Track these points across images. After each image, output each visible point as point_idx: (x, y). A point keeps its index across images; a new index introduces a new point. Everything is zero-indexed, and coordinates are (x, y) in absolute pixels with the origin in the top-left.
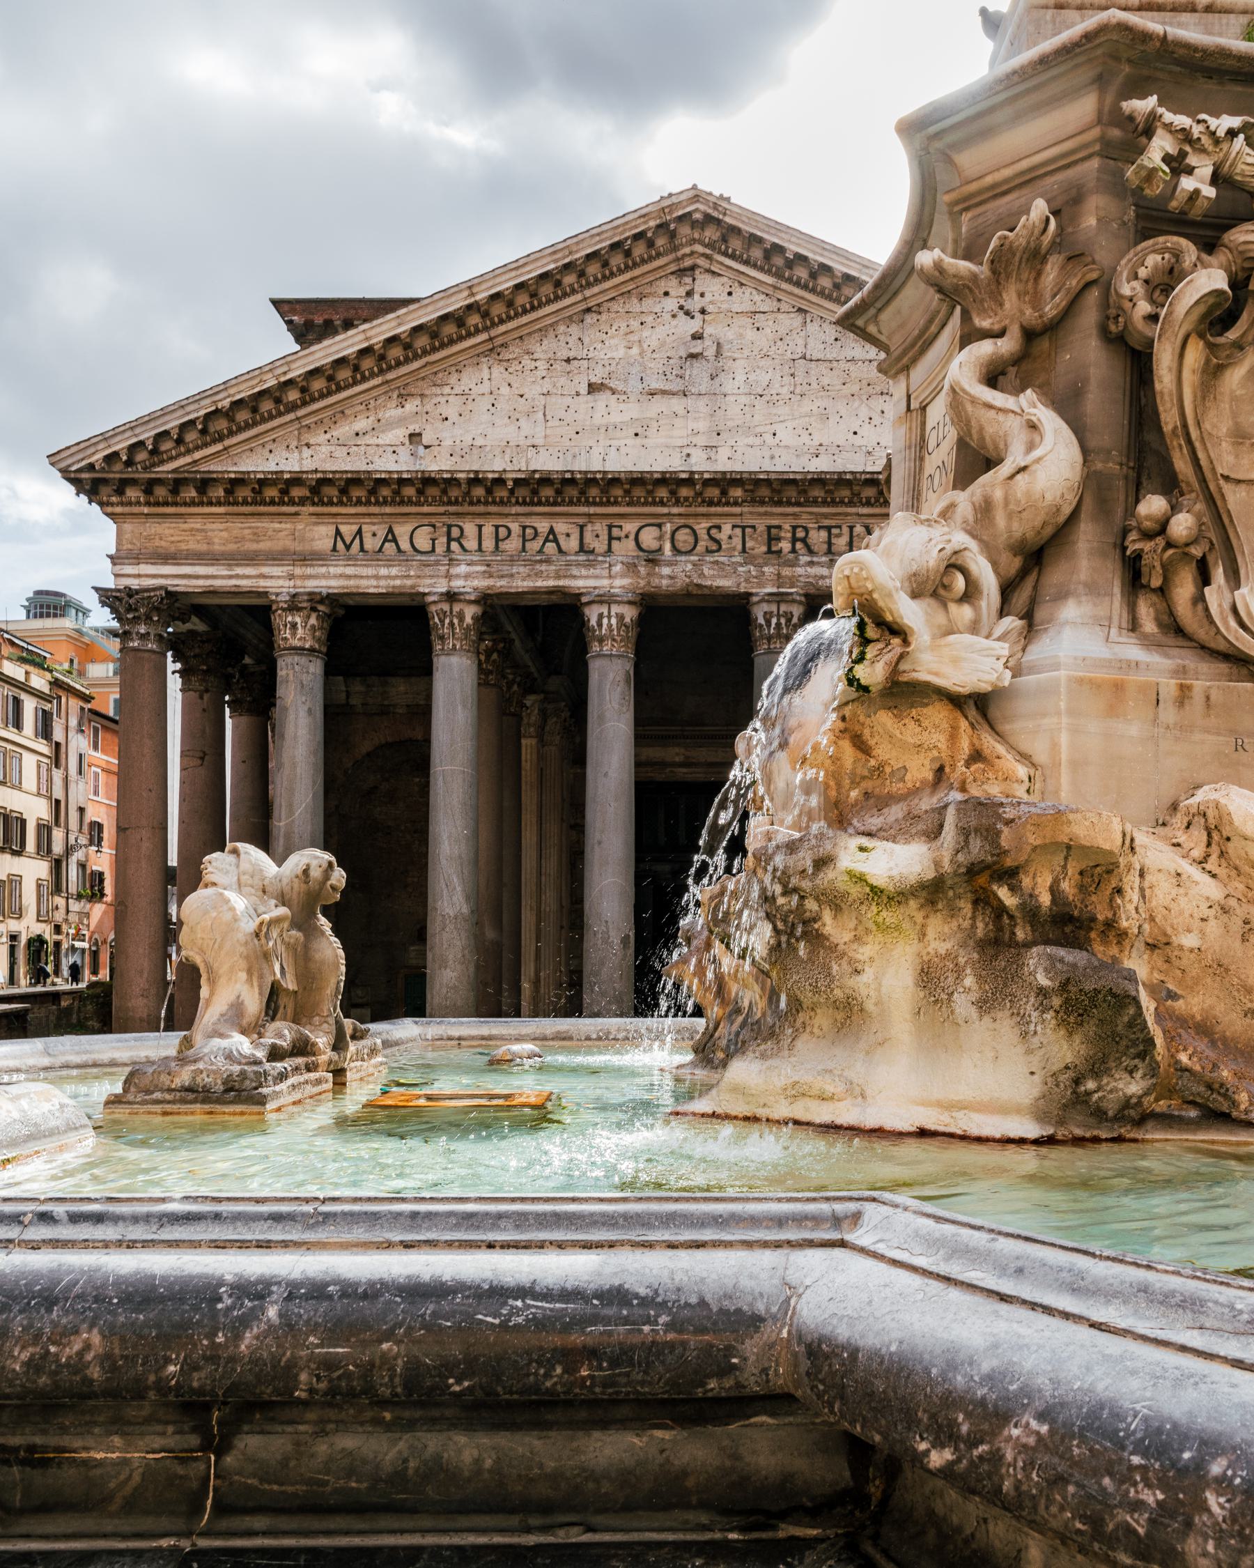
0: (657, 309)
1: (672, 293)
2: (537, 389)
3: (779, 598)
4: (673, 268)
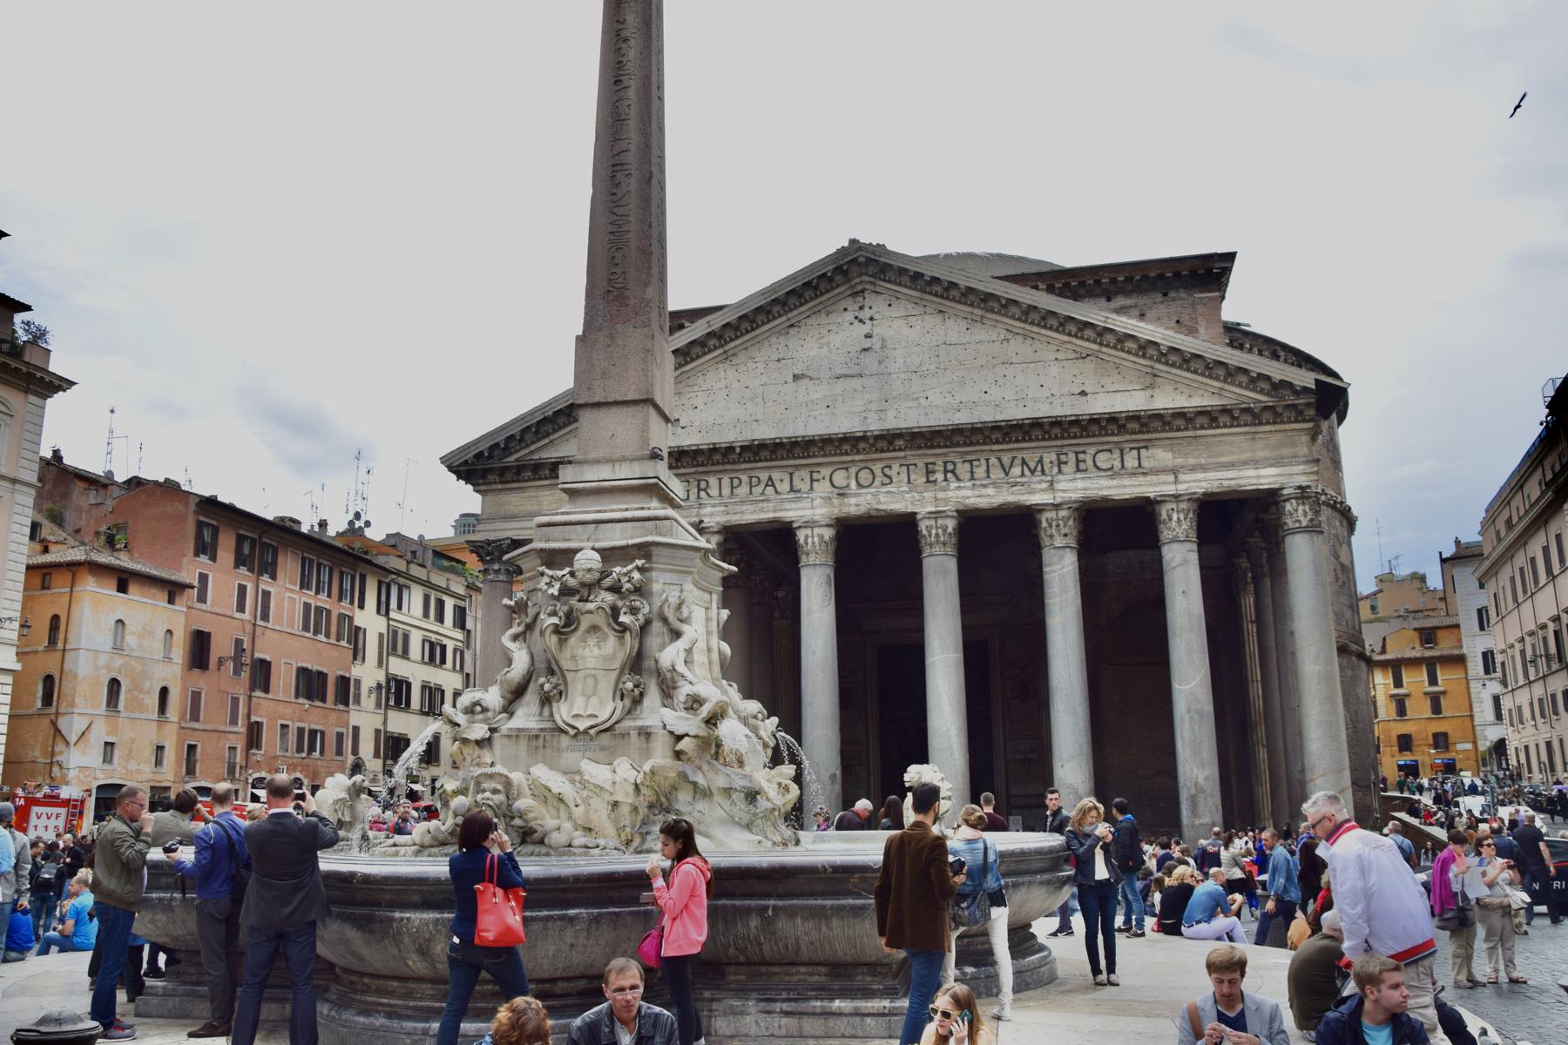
0: (840, 320)
1: (849, 308)
3: (937, 515)
4: (850, 292)
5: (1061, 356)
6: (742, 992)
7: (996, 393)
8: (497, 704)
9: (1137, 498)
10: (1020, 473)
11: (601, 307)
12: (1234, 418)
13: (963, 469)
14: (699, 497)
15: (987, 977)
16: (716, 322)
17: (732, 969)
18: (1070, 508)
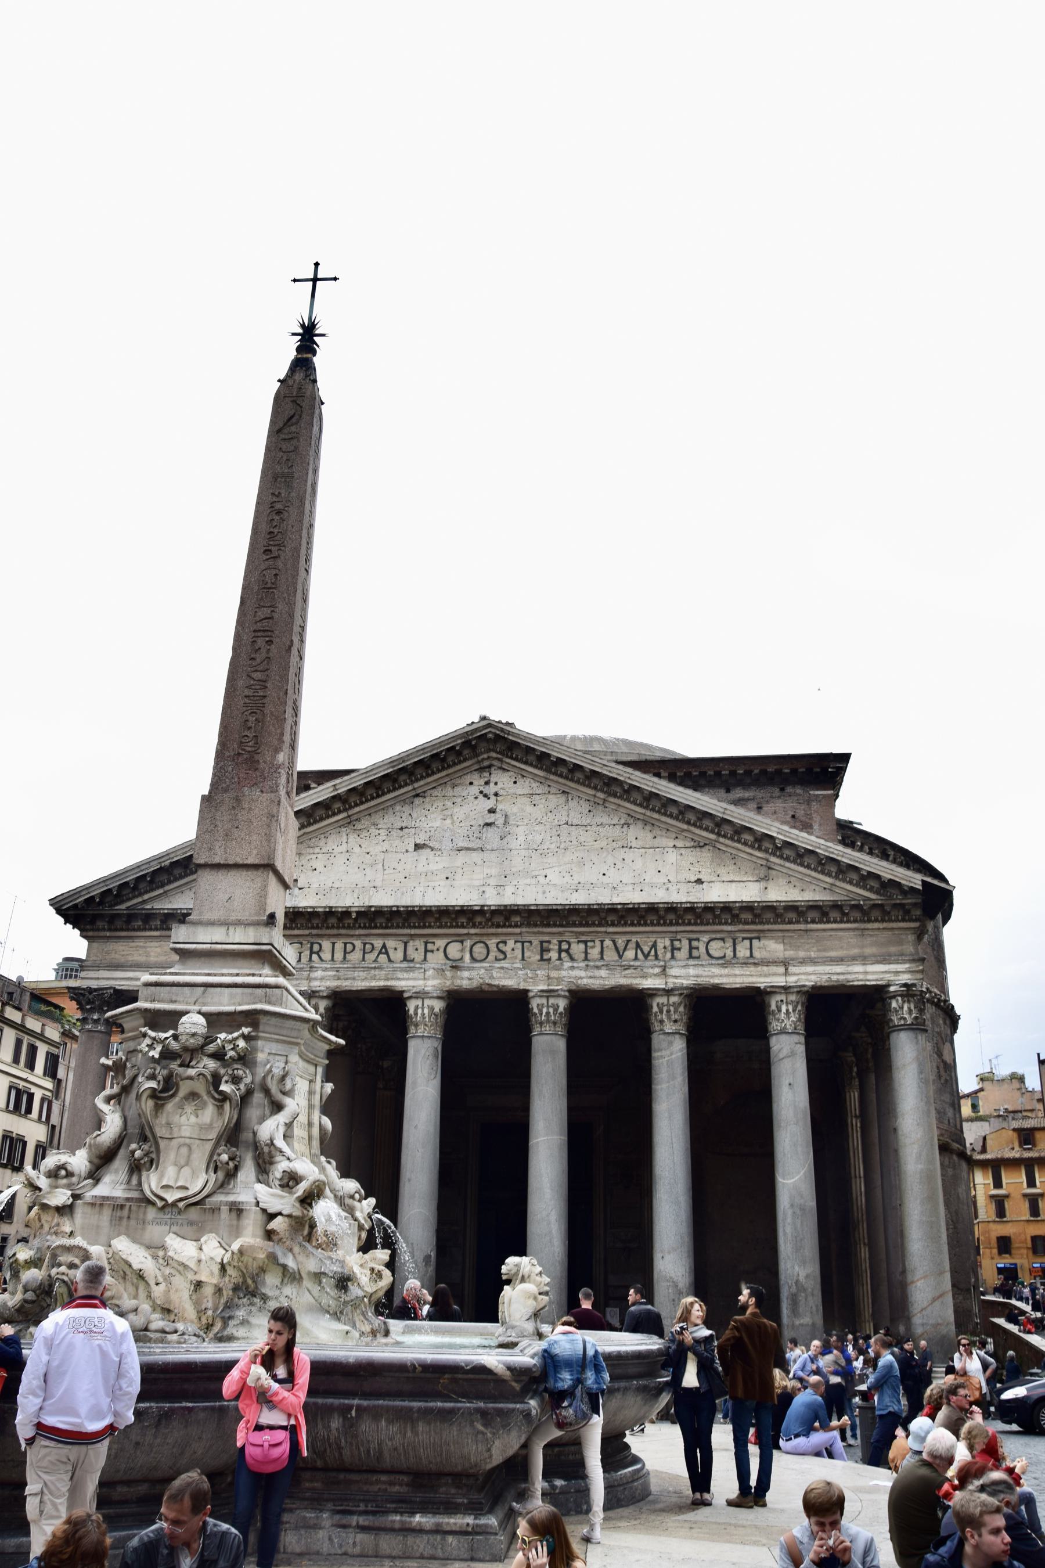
0: (465, 793)
1: (475, 783)
2: (379, 848)
3: (549, 994)
4: (476, 767)
5: (679, 844)
6: (316, 1502)
7: (613, 876)
8: (83, 1169)
9: (747, 988)
10: (633, 956)
11: (230, 769)
12: (844, 914)
13: (577, 949)
14: (310, 959)
15: (578, 1491)
16: (343, 785)
17: (308, 1475)
18: (681, 994)
